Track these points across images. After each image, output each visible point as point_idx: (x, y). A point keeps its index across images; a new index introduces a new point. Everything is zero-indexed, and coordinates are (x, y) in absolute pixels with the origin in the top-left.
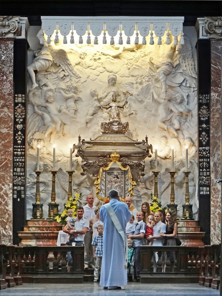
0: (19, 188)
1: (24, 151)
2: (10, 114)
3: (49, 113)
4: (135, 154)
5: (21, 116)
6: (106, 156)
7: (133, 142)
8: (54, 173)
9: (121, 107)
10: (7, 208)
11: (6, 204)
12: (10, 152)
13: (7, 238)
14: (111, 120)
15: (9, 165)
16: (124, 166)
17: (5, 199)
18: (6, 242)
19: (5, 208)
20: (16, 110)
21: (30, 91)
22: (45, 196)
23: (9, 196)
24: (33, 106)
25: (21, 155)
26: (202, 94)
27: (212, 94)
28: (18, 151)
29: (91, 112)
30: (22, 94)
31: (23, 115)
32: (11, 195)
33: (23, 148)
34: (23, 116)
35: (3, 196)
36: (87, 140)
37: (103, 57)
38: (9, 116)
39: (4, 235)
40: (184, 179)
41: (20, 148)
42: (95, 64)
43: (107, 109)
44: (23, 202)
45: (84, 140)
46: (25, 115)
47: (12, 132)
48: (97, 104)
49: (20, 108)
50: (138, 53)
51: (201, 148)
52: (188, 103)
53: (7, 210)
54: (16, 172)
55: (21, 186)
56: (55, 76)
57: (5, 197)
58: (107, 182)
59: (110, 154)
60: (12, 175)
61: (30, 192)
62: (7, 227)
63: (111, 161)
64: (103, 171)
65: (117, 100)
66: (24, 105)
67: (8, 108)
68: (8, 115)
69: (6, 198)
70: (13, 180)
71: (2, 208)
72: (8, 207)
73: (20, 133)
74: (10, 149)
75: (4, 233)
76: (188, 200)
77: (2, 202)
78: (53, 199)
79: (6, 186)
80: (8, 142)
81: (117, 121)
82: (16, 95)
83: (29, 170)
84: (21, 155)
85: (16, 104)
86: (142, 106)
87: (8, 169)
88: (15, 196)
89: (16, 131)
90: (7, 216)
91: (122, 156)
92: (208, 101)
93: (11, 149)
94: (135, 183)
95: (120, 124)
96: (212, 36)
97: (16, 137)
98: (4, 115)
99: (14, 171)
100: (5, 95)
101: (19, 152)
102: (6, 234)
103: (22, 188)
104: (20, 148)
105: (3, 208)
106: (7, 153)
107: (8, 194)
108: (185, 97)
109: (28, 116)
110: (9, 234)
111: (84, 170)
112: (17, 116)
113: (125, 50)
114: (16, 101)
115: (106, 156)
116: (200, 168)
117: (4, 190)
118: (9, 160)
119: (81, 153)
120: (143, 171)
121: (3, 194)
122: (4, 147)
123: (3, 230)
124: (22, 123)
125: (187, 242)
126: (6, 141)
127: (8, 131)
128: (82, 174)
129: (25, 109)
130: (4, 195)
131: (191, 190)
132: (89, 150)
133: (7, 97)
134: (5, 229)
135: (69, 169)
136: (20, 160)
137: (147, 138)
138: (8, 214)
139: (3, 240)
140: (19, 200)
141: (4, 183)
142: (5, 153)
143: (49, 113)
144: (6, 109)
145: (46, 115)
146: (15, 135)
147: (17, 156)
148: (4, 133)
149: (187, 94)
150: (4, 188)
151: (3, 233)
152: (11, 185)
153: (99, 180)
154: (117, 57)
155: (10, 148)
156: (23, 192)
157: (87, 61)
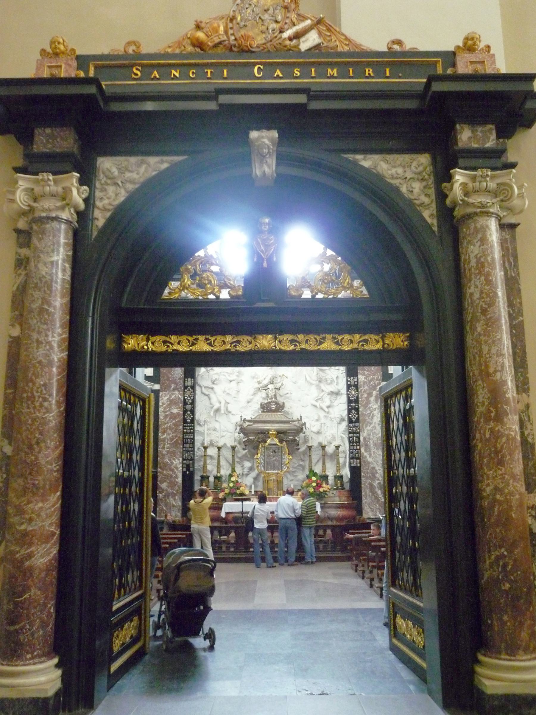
0: (188, 462)
1: (193, 429)
2: (180, 396)
4: (290, 430)
5: (190, 397)
6: (265, 434)
7: (288, 420)
8: (219, 448)
9: (277, 389)
10: (177, 480)
11: (176, 477)
14: (269, 400)
16: (281, 441)
19: (175, 481)
21: (198, 375)
22: (211, 468)
24: (201, 387)
25: (190, 433)
26: (350, 377)
27: (359, 376)
28: (186, 429)
29: (252, 392)
30: (191, 378)
32: (181, 468)
33: (191, 426)
34: (192, 398)
36: (248, 418)
38: (179, 398)
39: (174, 506)
40: (335, 452)
43: (266, 390)
44: (192, 474)
45: (245, 419)
46: (194, 397)
47: (182, 413)
48: (257, 385)
49: (189, 390)
51: (351, 425)
52: (337, 384)
53: (177, 482)
54: (185, 447)
55: (190, 460)
58: (266, 457)
59: (268, 431)
60: (182, 450)
61: (198, 465)
62: (177, 498)
63: (269, 438)
64: (263, 446)
65: (275, 382)
66: (193, 387)
67: (179, 391)
70: (183, 455)
73: (189, 413)
75: (174, 503)
76: (338, 470)
78: (218, 471)
79: (177, 460)
80: (178, 421)
81: (274, 402)
82: (186, 379)
83: (198, 444)
85: (186, 387)
88: (185, 469)
89: (185, 411)
90: (177, 488)
91: (279, 433)
92: (356, 383)
93: (181, 427)
94: (291, 457)
95: (276, 403)
99: (183, 447)
100: (176, 380)
103: (191, 462)
108: (335, 379)
109: (197, 397)
111: (246, 446)
114: (186, 385)
115: (265, 433)
116: (350, 442)
118: (179, 437)
119: (243, 430)
120: (298, 445)
122: (175, 426)
124: (191, 404)
125: (341, 511)
128: (244, 449)
129: (194, 392)
131: (341, 461)
132: (250, 427)
133: (178, 381)
134: (175, 499)
135: (233, 445)
136: (189, 437)
137: (301, 416)
138: (178, 486)
140: (188, 473)
142: (176, 431)
143: (215, 393)
144: (176, 392)
145: (212, 396)
147: (187, 433)
149: (336, 376)
150: (175, 463)
152: (181, 459)
153: (259, 455)
156: (191, 466)
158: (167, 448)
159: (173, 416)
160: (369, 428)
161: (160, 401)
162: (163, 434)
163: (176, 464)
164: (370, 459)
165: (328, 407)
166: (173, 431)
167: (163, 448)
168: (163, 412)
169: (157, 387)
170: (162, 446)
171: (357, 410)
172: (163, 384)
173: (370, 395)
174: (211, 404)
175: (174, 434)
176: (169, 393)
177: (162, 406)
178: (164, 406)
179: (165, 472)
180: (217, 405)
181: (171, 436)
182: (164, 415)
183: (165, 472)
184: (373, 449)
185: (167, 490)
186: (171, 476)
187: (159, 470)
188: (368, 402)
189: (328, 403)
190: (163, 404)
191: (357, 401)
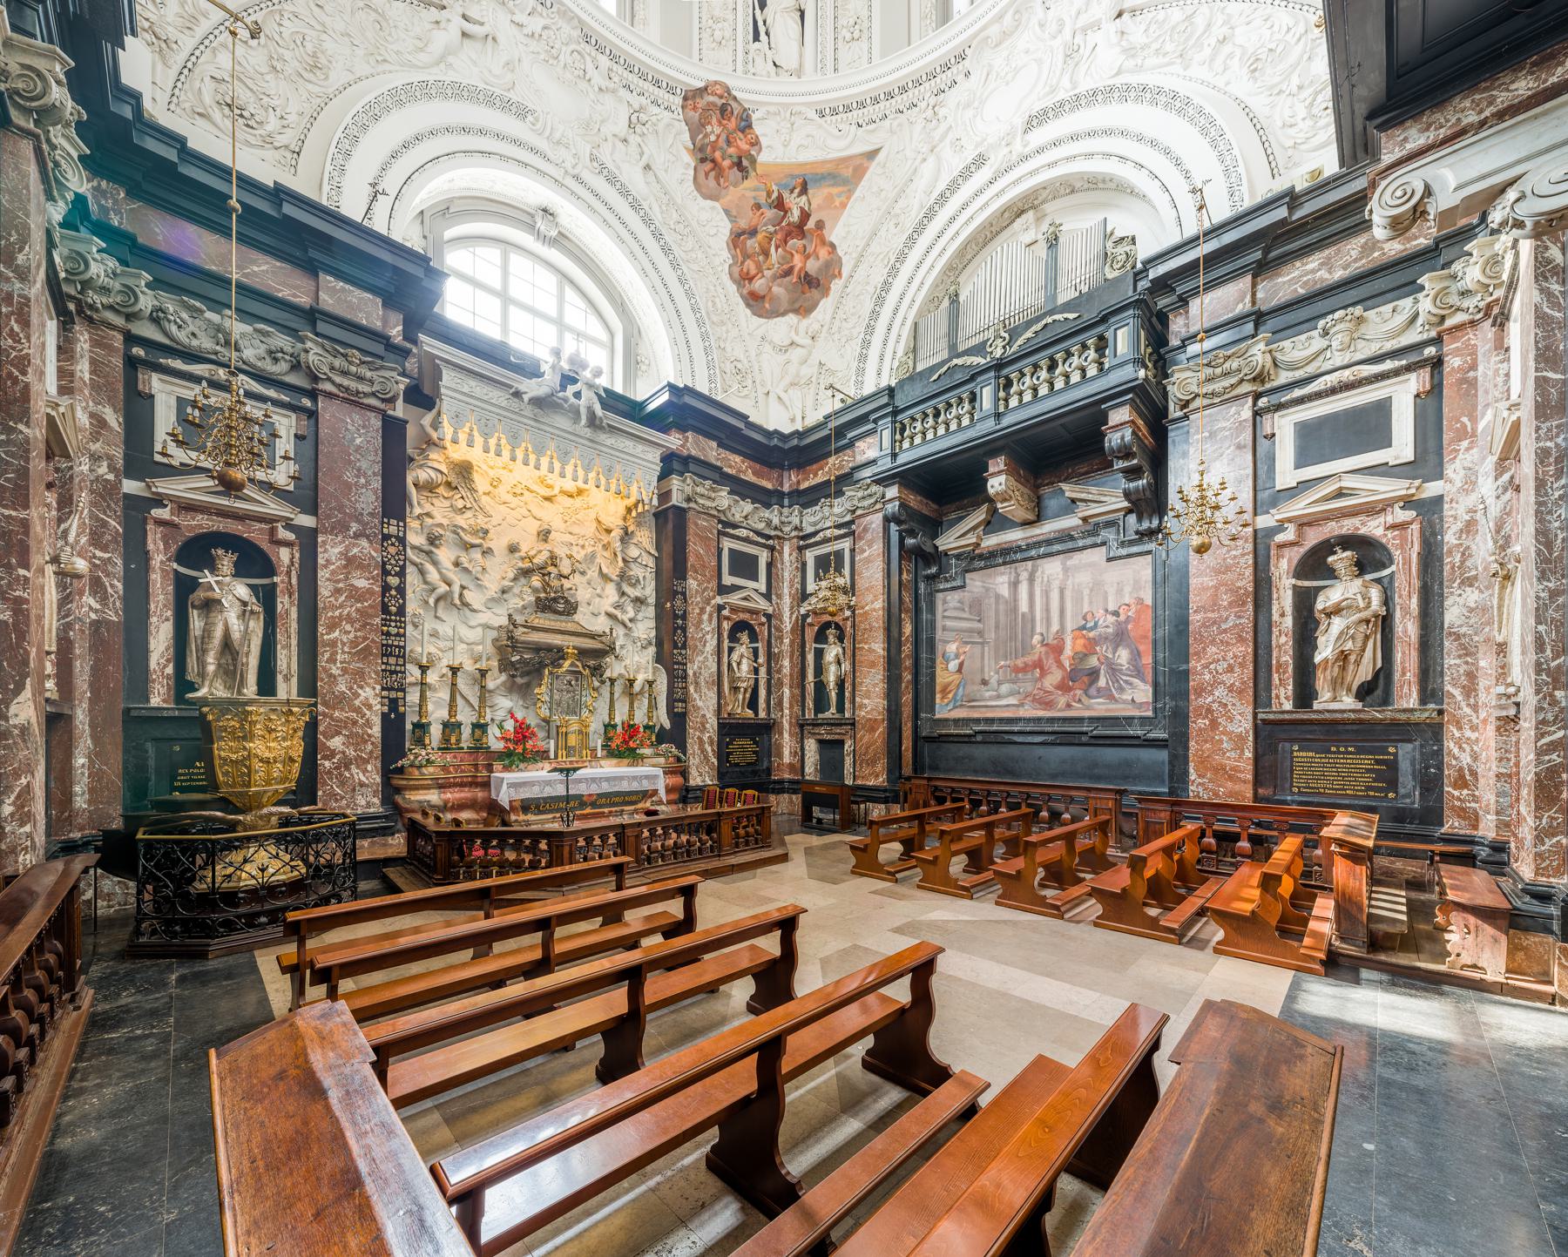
3: (435, 563)
25: (398, 635)
37: (527, 493)
42: (515, 501)
47: (378, 589)
50: (578, 502)
56: (447, 503)
67: (370, 542)
73: (393, 592)
84: (398, 635)
86: (584, 579)
89: (386, 588)
91: (583, 653)
93: (378, 621)
96: (692, 505)
113: (563, 492)
143: (435, 563)
144: (364, 543)
145: (429, 567)
146: (383, 596)
154: (548, 499)
157: (502, 492)
159: (356, 595)
160: (700, 659)
164: (700, 703)
165: (631, 620)
171: (684, 630)
172: (328, 517)
173: (702, 610)
174: (426, 582)
177: (326, 566)
180: (443, 588)
182: (331, 587)
184: (704, 690)
188: (700, 622)
189: (631, 614)
191: (684, 617)
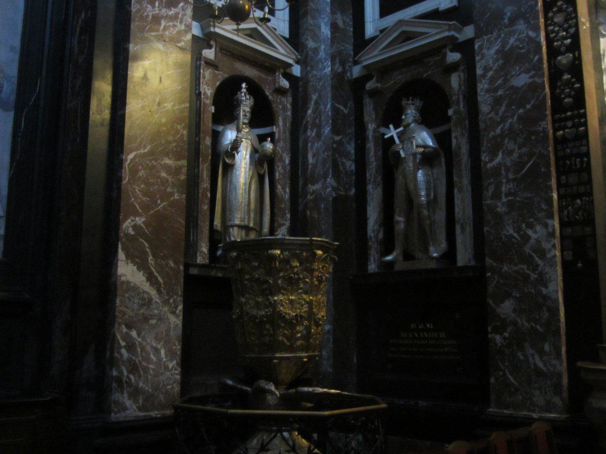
5: (566, 30)
10: (544, 291)
11: (542, 280)
12: (542, 135)
13: (549, 382)
15: (543, 170)
17: (538, 266)
18: (546, 393)
20: (552, 18)
23: (548, 256)
28: (563, 128)
31: (570, 27)
34: (572, 31)
35: (532, 256)
39: (539, 373)
41: (572, 118)
49: (560, 10)
57: (537, 259)
62: (547, 347)
68: (528, 36)
69: (540, 262)
71: (530, 292)
72: (546, 287)
73: (566, 77)
74: (540, 126)
75: (540, 365)
77: (529, 276)
79: (538, 228)
87: (540, 181)
88: (569, 256)
89: (555, 74)
90: (546, 315)
97: (558, 91)
98: (518, 40)
101: (570, 128)
102: (545, 369)
103: (588, 230)
104: (572, 118)
105: (533, 291)
106: (533, 138)
107: (544, 250)
110: (552, 369)
112: (554, 34)
117: (532, 241)
121: (531, 253)
123: (537, 358)
126: (528, 107)
127: (531, 80)
130: (534, 255)
134: (541, 353)
139: (536, 386)
140: (580, 265)
141: (532, 220)
148: (523, 86)
150: (534, 236)
151: (535, 364)
155: (540, 123)
158: (507, 195)
159: (517, 97)
161: (478, 65)
162: (494, 155)
163: (538, 241)
166: (520, 140)
167: (497, 195)
168: (487, 91)
169: (469, 32)
170: (491, 189)
175: (524, 150)
176: (499, 36)
178: (490, 74)
179: (505, 268)
181: (515, 155)
183: (505, 268)
185: (515, 324)
186: (526, 278)
187: (488, 261)
190: (486, 69)
